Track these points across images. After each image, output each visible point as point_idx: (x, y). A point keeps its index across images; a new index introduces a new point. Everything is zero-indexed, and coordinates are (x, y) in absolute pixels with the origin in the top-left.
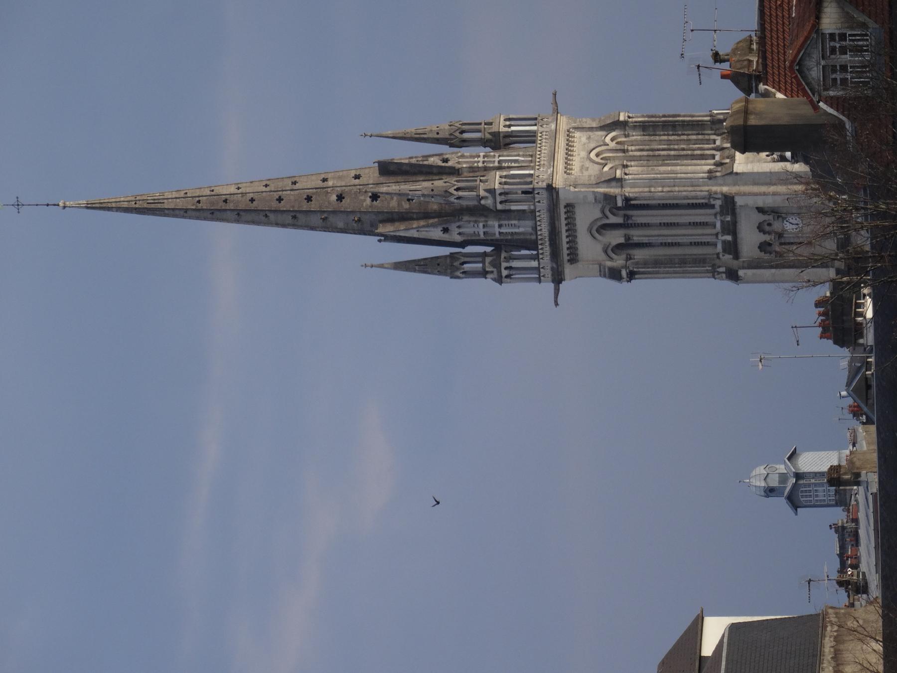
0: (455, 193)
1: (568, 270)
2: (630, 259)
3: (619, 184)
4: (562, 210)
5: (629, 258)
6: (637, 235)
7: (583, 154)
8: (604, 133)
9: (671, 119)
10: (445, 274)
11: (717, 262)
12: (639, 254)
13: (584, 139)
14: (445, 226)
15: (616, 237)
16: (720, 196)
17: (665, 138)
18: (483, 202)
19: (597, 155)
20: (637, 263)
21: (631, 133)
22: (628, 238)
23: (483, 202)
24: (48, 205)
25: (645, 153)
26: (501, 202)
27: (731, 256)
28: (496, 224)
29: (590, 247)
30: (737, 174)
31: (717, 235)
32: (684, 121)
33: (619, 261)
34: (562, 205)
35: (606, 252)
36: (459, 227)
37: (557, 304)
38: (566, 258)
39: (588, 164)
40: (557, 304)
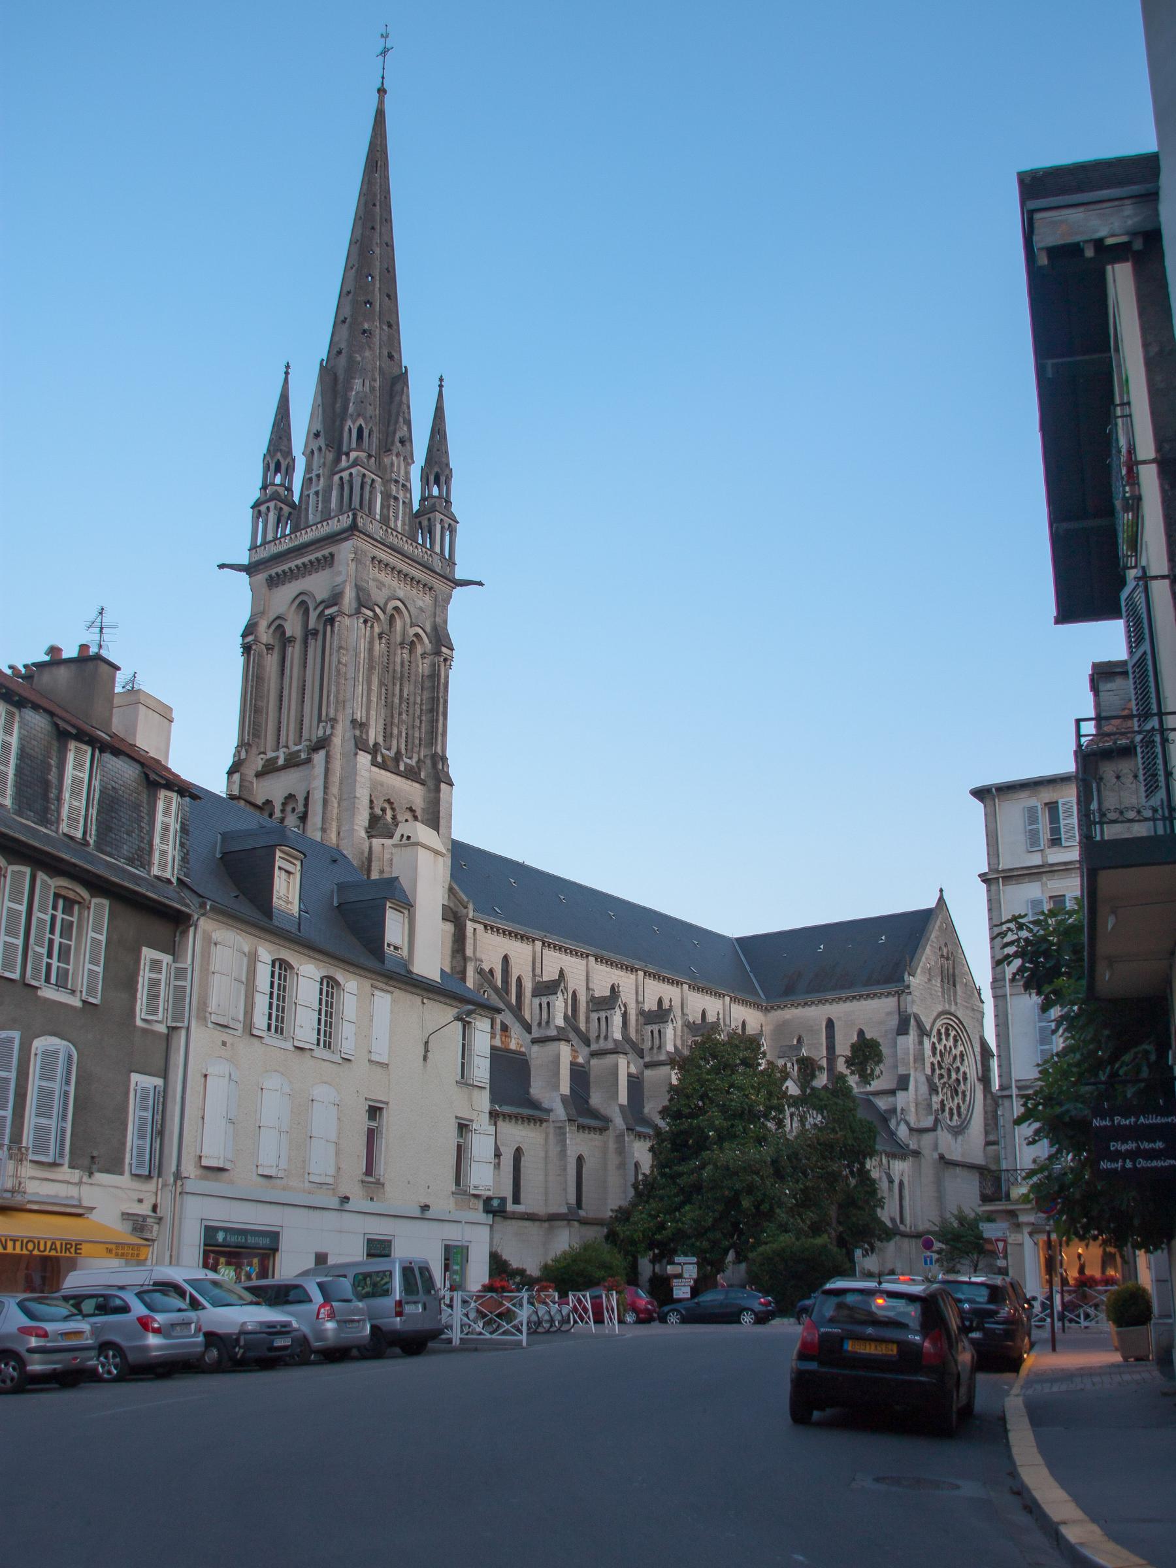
0: (357, 425)
1: (261, 577)
2: (268, 649)
3: (353, 612)
4: (326, 552)
5: (269, 648)
6: (294, 652)
7: (401, 594)
8: (428, 629)
9: (441, 709)
10: (268, 450)
11: (254, 750)
12: (271, 662)
13: (420, 603)
14: (322, 434)
15: (293, 627)
16: (328, 732)
17: (418, 700)
18: (344, 457)
19: (396, 609)
20: (260, 655)
21: (425, 661)
22: (291, 640)
23: (344, 457)
24: (382, 91)
25: (398, 668)
26: (341, 478)
27: (260, 768)
28: (320, 488)
29: (283, 598)
30: (356, 754)
31: (287, 747)
32: (437, 721)
33: (265, 635)
34: (332, 549)
35: (278, 618)
36: (320, 449)
37: (221, 566)
38: (273, 572)
39: (385, 593)
40: (221, 566)
